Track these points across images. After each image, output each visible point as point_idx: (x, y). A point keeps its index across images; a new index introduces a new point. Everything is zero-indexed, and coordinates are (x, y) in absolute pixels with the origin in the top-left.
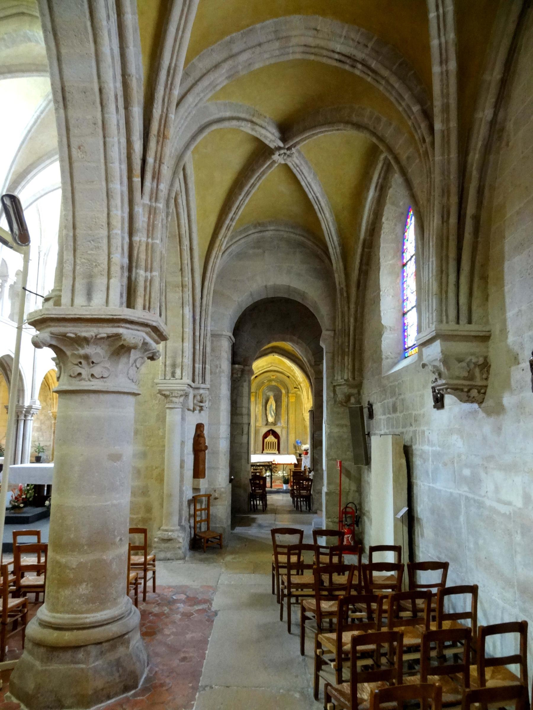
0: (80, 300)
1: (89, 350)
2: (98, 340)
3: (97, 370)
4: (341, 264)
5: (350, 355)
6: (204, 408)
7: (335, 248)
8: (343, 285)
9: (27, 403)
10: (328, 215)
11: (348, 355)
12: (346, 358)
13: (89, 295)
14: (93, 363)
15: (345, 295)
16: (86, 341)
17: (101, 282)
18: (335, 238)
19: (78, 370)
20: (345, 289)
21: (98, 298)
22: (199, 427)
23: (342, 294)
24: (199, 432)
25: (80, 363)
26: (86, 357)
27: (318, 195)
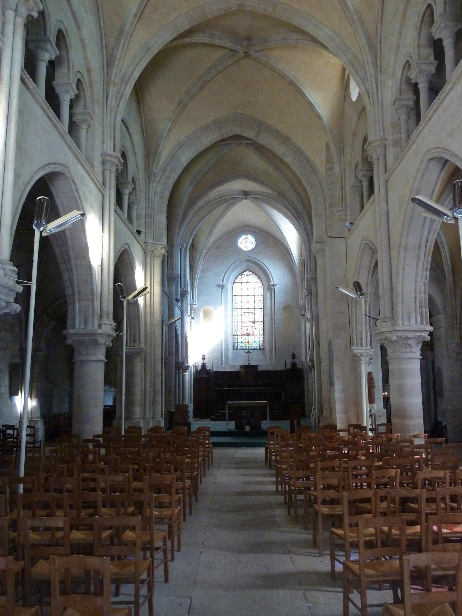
0: (406, 323)
1: (410, 342)
2: (414, 338)
3: (413, 350)
4: (451, 275)
5: (458, 330)
6: (372, 363)
7: (448, 267)
8: (452, 288)
9: (180, 361)
10: (447, 250)
11: (457, 329)
12: (455, 330)
13: (409, 321)
14: (411, 347)
15: (453, 293)
16: (410, 338)
17: (413, 315)
18: (449, 261)
19: (406, 350)
20: (453, 289)
21: (413, 322)
22: (370, 374)
23: (451, 293)
24: (370, 377)
25: (407, 347)
26: (409, 345)
27: (443, 240)
